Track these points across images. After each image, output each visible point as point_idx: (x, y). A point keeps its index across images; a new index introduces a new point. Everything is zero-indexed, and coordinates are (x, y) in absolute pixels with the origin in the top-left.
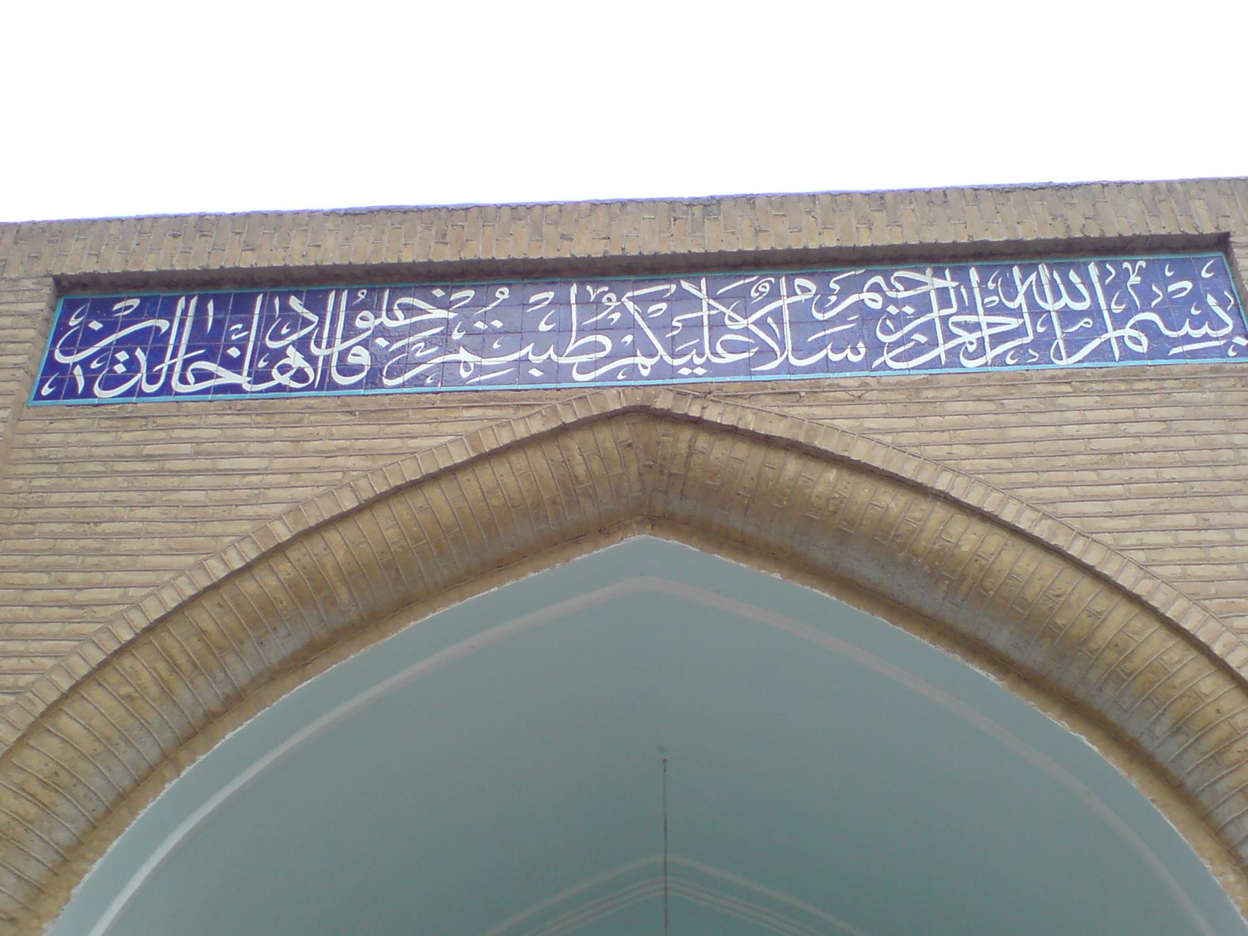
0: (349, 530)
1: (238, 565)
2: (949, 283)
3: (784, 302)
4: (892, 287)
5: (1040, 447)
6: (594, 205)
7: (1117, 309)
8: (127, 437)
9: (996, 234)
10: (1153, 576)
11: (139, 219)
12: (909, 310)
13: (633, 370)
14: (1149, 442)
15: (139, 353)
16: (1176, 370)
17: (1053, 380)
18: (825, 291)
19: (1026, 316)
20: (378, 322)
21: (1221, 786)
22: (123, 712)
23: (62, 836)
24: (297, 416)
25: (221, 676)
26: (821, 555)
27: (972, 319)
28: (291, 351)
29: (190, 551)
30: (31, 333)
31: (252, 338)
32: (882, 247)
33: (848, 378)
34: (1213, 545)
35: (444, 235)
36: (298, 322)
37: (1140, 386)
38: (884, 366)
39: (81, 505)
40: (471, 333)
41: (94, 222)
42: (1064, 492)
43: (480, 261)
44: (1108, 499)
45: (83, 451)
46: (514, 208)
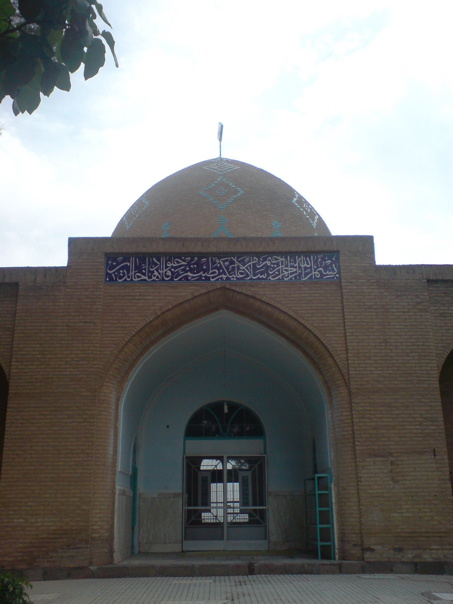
3: (251, 263)
12: (275, 266)
13: (222, 278)
18: (259, 261)
28: (155, 271)
33: (263, 282)
36: (156, 264)
38: (270, 279)
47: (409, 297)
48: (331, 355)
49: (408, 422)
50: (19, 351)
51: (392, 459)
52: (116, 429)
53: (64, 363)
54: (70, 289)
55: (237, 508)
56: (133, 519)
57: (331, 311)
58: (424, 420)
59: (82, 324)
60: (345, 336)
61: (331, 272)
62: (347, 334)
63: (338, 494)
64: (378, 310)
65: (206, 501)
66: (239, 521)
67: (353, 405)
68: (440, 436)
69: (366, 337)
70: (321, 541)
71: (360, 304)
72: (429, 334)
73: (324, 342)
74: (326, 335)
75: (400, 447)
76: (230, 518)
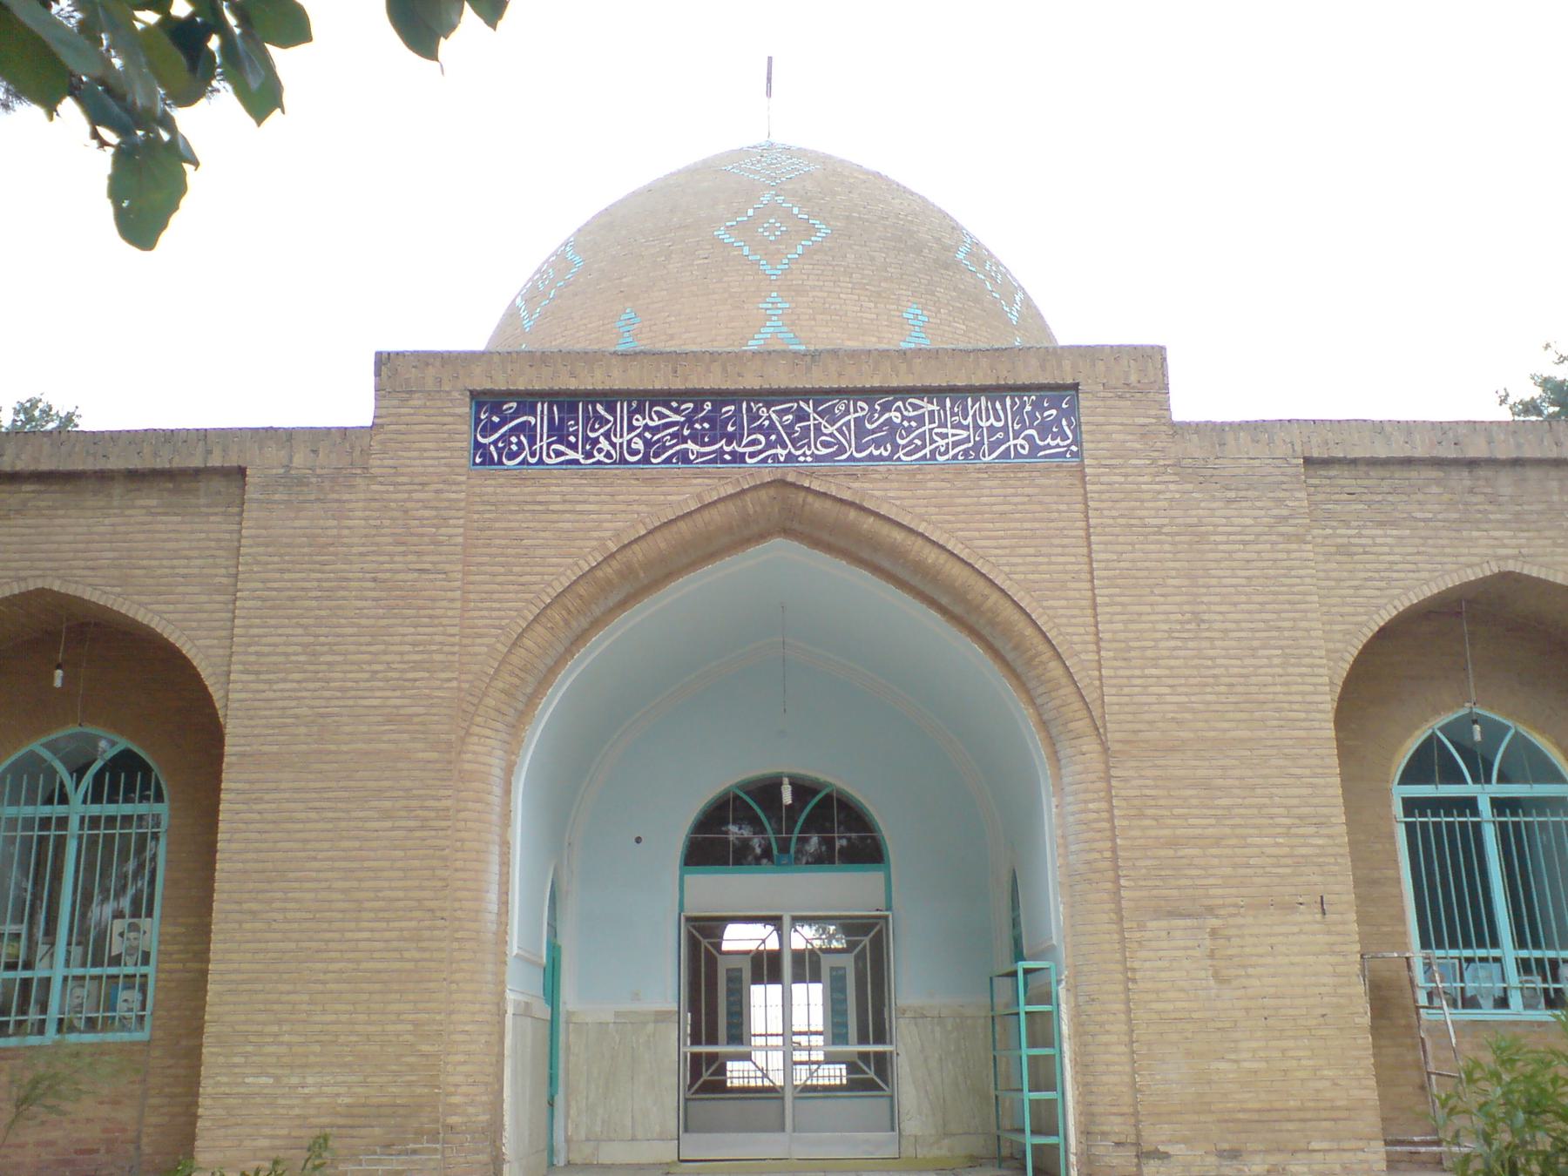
0: (643, 544)
3: (851, 417)
8: (527, 490)
9: (960, 382)
12: (913, 424)
13: (775, 457)
17: (979, 470)
18: (872, 410)
23: (529, 690)
27: (944, 430)
29: (570, 556)
33: (882, 466)
34: (1041, 564)
38: (899, 459)
39: (512, 529)
47: (1259, 504)
48: (1059, 656)
49: (1255, 827)
50: (249, 645)
51: (1215, 922)
52: (505, 845)
53: (366, 675)
54: (381, 484)
55: (817, 1048)
56: (552, 1080)
57: (1056, 541)
58: (1297, 821)
59: (411, 576)
62: (1099, 600)
63: (1077, 1013)
64: (1177, 538)
65: (738, 1032)
66: (826, 1082)
67: (1114, 783)
68: (1336, 864)
69: (1148, 609)
70: (1033, 1132)
71: (1133, 522)
72: (1308, 598)
75: (1233, 891)
76: (801, 1076)
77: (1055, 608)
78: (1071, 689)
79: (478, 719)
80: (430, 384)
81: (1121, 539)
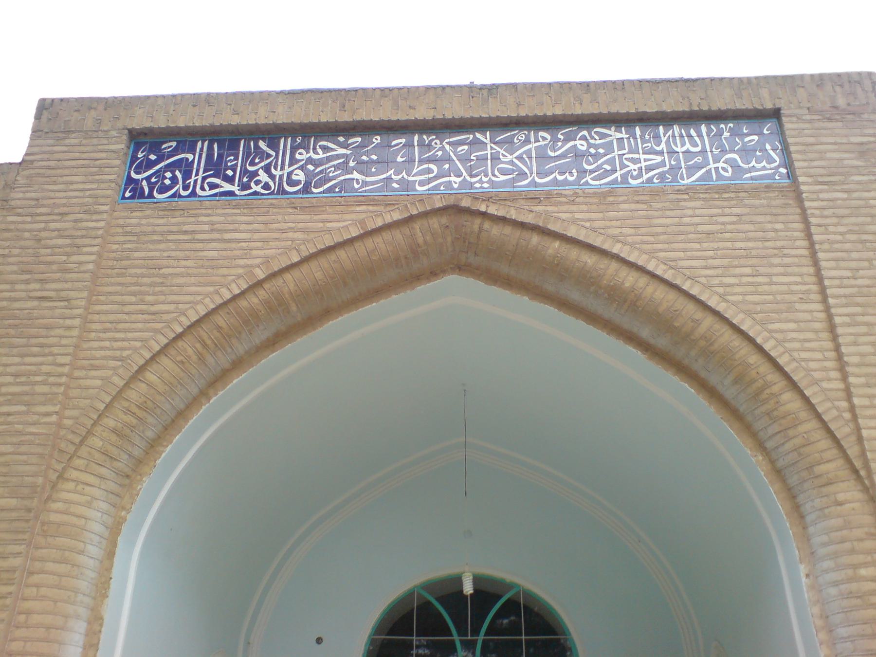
0: (296, 273)
1: (237, 291)
2: (624, 135)
4: (592, 138)
5: (669, 230)
6: (428, 89)
7: (716, 152)
8: (173, 220)
9: (651, 107)
10: (727, 301)
11: (174, 96)
12: (601, 151)
14: (729, 227)
15: (177, 173)
16: (746, 186)
17: (679, 192)
18: (555, 140)
19: (666, 155)
20: (308, 155)
21: (757, 412)
22: (179, 370)
23: (149, 434)
24: (265, 210)
25: (229, 350)
26: (550, 287)
27: (636, 156)
28: (261, 172)
29: (212, 284)
30: (118, 162)
31: (239, 165)
32: (588, 115)
34: (760, 284)
35: (344, 106)
36: (265, 156)
37: (726, 195)
38: (587, 183)
39: (151, 258)
40: (360, 163)
41: (148, 97)
42: (681, 254)
43: (364, 121)
44: (706, 258)
45: (150, 229)
46: (382, 90)
48: (794, 386)
52: (96, 621)
54: (19, 215)
57: (776, 261)
59: (30, 304)
60: (832, 328)
61: (764, 163)
62: (838, 320)
71: (865, 237)
73: (767, 347)
74: (771, 327)
77: (782, 331)
78: (813, 424)
79: (78, 462)
80: (89, 124)
81: (854, 255)
